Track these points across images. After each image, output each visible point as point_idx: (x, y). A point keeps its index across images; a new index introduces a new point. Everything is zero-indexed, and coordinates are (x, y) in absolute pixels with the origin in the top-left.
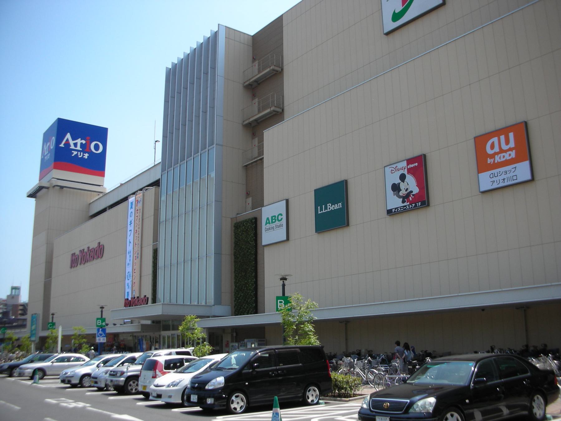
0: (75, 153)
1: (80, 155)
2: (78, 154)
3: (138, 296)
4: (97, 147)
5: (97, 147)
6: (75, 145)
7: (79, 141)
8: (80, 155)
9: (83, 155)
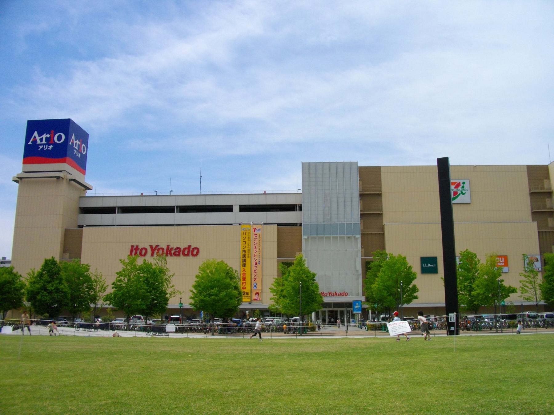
0: (41, 147)
1: (46, 148)
2: (43, 147)
3: (357, 258)
4: (59, 138)
5: (59, 138)
6: (41, 140)
7: (44, 136)
8: (46, 148)
9: (48, 147)
